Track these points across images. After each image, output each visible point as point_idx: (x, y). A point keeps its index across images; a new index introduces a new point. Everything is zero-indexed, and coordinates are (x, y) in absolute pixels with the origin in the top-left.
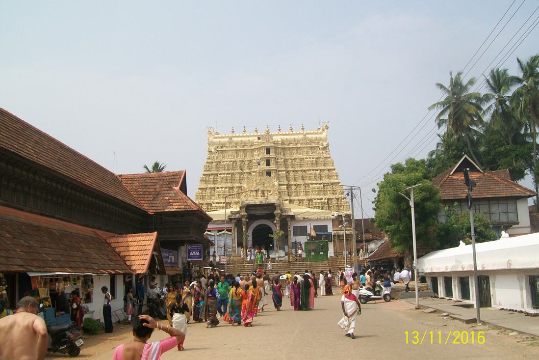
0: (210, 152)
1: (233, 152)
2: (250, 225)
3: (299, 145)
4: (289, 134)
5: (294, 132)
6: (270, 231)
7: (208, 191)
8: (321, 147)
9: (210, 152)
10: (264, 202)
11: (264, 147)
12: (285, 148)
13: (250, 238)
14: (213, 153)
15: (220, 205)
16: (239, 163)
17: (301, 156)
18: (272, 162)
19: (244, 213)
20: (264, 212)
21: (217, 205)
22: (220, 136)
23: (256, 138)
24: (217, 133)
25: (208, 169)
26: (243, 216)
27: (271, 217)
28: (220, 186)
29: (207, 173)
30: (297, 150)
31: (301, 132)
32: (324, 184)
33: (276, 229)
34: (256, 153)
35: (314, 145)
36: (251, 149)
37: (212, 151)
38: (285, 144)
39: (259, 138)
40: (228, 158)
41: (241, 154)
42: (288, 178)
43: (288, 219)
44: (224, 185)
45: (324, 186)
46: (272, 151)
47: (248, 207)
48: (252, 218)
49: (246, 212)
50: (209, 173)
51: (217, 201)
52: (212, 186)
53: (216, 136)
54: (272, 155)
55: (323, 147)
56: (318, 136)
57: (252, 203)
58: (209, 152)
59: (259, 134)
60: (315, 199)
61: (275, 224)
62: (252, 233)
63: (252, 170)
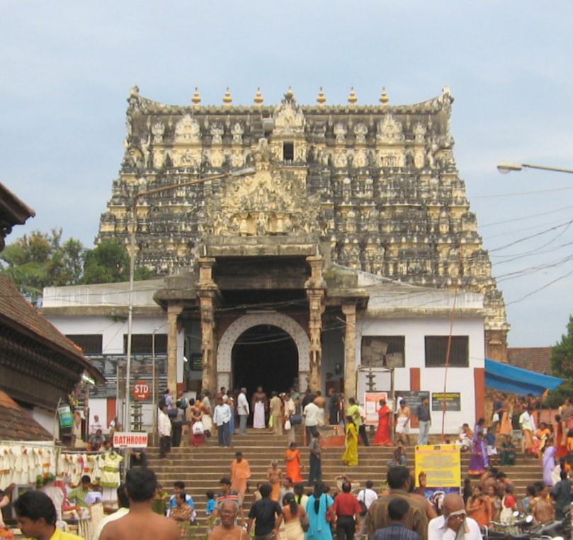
2: (226, 328)
6: (289, 352)
11: (278, 138)
13: (224, 363)
19: (206, 279)
26: (203, 294)
33: (308, 347)
43: (349, 311)
47: (225, 266)
48: (231, 303)
49: (216, 275)
62: (233, 349)
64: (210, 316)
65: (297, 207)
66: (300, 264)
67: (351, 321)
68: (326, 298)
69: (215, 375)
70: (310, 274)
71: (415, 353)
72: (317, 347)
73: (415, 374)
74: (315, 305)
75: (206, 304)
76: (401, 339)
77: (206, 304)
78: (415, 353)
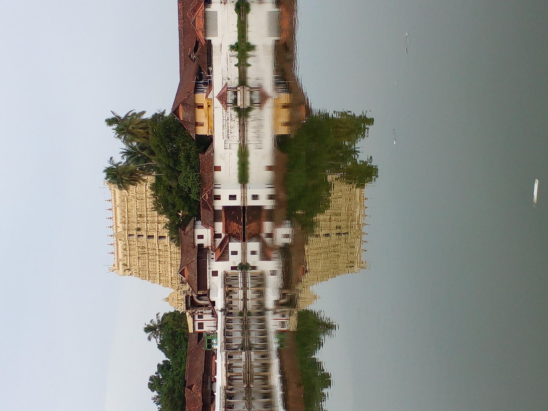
0: (131, 274)
3: (126, 211)
7: (162, 278)
9: (131, 274)
10: (185, 301)
15: (173, 271)
16: (140, 256)
17: (135, 210)
18: (140, 233)
21: (173, 274)
22: (116, 265)
23: (119, 242)
24: (114, 265)
25: (144, 278)
28: (158, 270)
29: (148, 279)
34: (132, 243)
35: (126, 200)
40: (136, 264)
41: (132, 252)
42: (153, 222)
44: (158, 267)
46: (131, 233)
50: (148, 277)
51: (170, 273)
52: (158, 276)
53: (117, 268)
54: (134, 232)
56: (117, 196)
57: (185, 308)
66: (187, 297)
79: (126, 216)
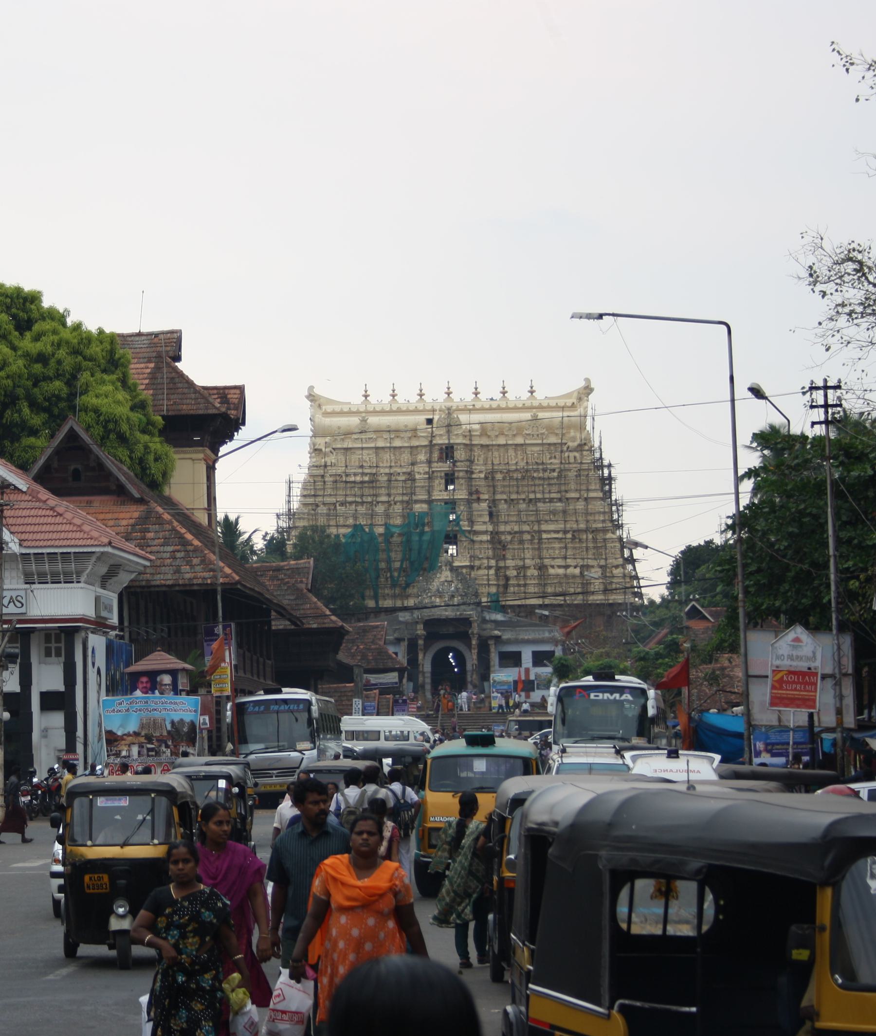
0: (316, 451)
1: (371, 452)
3: (519, 440)
4: (499, 409)
5: (511, 405)
8: (570, 444)
12: (487, 446)
14: (325, 455)
19: (420, 630)
20: (451, 630)
22: (338, 408)
23: (422, 418)
27: (465, 637)
30: (516, 451)
31: (528, 404)
32: (574, 531)
33: (472, 659)
36: (411, 447)
37: (321, 450)
38: (489, 437)
39: (430, 421)
43: (491, 642)
45: (573, 535)
47: (429, 623)
49: (424, 629)
53: (329, 408)
55: (576, 444)
58: (316, 450)
59: (429, 407)
60: (553, 567)
61: (469, 646)
63: (414, 498)
64: (422, 647)
65: (464, 589)
66: (466, 622)
67: (492, 649)
68: (480, 637)
69: (423, 673)
70: (471, 626)
71: (527, 659)
72: (476, 662)
73: (527, 671)
74: (474, 642)
75: (421, 642)
76: (519, 654)
77: (421, 642)
78: (527, 659)
79: (502, 441)
